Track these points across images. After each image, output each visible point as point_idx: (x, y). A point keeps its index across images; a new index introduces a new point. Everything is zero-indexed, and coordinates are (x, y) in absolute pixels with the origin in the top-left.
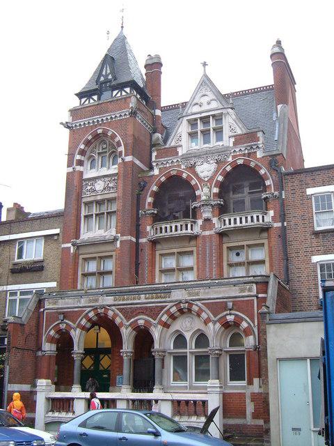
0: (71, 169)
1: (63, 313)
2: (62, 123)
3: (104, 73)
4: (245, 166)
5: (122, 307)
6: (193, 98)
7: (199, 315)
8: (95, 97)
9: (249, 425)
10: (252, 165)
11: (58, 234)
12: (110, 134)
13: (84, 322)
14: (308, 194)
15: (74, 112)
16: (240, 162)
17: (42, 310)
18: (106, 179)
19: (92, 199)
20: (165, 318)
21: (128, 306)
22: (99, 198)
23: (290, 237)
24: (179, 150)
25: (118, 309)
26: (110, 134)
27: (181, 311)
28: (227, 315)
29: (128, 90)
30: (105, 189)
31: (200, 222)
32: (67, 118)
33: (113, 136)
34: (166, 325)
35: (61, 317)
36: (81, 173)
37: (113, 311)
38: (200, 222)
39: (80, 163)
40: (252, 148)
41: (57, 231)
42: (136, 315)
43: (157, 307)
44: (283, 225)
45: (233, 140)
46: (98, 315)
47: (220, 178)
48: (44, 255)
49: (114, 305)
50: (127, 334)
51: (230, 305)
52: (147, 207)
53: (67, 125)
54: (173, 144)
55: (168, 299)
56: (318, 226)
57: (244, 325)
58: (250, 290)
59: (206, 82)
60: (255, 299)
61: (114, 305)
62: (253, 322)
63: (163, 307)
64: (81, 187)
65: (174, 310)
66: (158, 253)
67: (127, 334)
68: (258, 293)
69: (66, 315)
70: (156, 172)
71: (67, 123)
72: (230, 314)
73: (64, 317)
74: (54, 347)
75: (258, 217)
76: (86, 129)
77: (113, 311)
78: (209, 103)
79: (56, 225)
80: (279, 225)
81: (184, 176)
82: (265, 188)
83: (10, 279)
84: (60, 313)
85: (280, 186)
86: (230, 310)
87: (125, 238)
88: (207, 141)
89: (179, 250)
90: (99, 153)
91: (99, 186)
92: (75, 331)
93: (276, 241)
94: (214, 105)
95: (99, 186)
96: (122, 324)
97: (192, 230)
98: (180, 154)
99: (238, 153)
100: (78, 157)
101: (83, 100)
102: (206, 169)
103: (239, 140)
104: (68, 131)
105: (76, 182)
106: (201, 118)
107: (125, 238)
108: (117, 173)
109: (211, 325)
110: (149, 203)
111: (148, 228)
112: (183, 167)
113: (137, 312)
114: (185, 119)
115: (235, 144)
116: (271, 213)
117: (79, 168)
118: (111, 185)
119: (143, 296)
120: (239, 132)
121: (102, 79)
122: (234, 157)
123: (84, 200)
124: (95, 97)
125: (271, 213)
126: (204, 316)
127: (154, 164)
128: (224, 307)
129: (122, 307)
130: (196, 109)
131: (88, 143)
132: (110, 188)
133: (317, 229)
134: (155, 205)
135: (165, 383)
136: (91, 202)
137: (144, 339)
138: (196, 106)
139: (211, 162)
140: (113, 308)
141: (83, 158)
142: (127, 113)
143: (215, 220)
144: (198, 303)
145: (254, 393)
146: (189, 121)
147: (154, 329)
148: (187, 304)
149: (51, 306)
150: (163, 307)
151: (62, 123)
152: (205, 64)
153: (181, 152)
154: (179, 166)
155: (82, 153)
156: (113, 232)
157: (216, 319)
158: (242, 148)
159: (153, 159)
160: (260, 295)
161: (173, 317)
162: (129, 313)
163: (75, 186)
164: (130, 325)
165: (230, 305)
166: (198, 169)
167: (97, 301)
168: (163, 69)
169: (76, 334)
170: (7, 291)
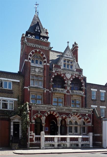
4: (78, 78)
7: (78, 116)
11: (19, 82)
13: (46, 115)
19: (34, 74)
21: (60, 112)
22: (37, 74)
23: (87, 99)
24: (61, 67)
26: (41, 53)
33: (43, 55)
35: (39, 112)
37: (56, 112)
38: (66, 90)
41: (19, 81)
42: (63, 115)
45: (76, 69)
47: (72, 79)
49: (56, 111)
54: (59, 64)
57: (89, 120)
58: (91, 112)
61: (56, 111)
63: (70, 113)
65: (73, 114)
66: (53, 96)
67: (60, 119)
77: (56, 112)
80: (85, 96)
81: (62, 75)
82: (82, 86)
87: (47, 90)
88: (68, 67)
89: (59, 97)
91: (37, 70)
92: (43, 117)
93: (84, 100)
98: (61, 68)
102: (68, 76)
107: (47, 90)
114: (63, 58)
122: (75, 75)
123: (31, 73)
126: (80, 117)
130: (65, 56)
133: (92, 99)
134: (53, 81)
136: (34, 75)
141: (31, 58)
146: (64, 59)
149: (34, 108)
154: (61, 72)
158: (77, 73)
159: (53, 67)
160: (92, 113)
161: (72, 116)
162: (61, 114)
166: (66, 75)
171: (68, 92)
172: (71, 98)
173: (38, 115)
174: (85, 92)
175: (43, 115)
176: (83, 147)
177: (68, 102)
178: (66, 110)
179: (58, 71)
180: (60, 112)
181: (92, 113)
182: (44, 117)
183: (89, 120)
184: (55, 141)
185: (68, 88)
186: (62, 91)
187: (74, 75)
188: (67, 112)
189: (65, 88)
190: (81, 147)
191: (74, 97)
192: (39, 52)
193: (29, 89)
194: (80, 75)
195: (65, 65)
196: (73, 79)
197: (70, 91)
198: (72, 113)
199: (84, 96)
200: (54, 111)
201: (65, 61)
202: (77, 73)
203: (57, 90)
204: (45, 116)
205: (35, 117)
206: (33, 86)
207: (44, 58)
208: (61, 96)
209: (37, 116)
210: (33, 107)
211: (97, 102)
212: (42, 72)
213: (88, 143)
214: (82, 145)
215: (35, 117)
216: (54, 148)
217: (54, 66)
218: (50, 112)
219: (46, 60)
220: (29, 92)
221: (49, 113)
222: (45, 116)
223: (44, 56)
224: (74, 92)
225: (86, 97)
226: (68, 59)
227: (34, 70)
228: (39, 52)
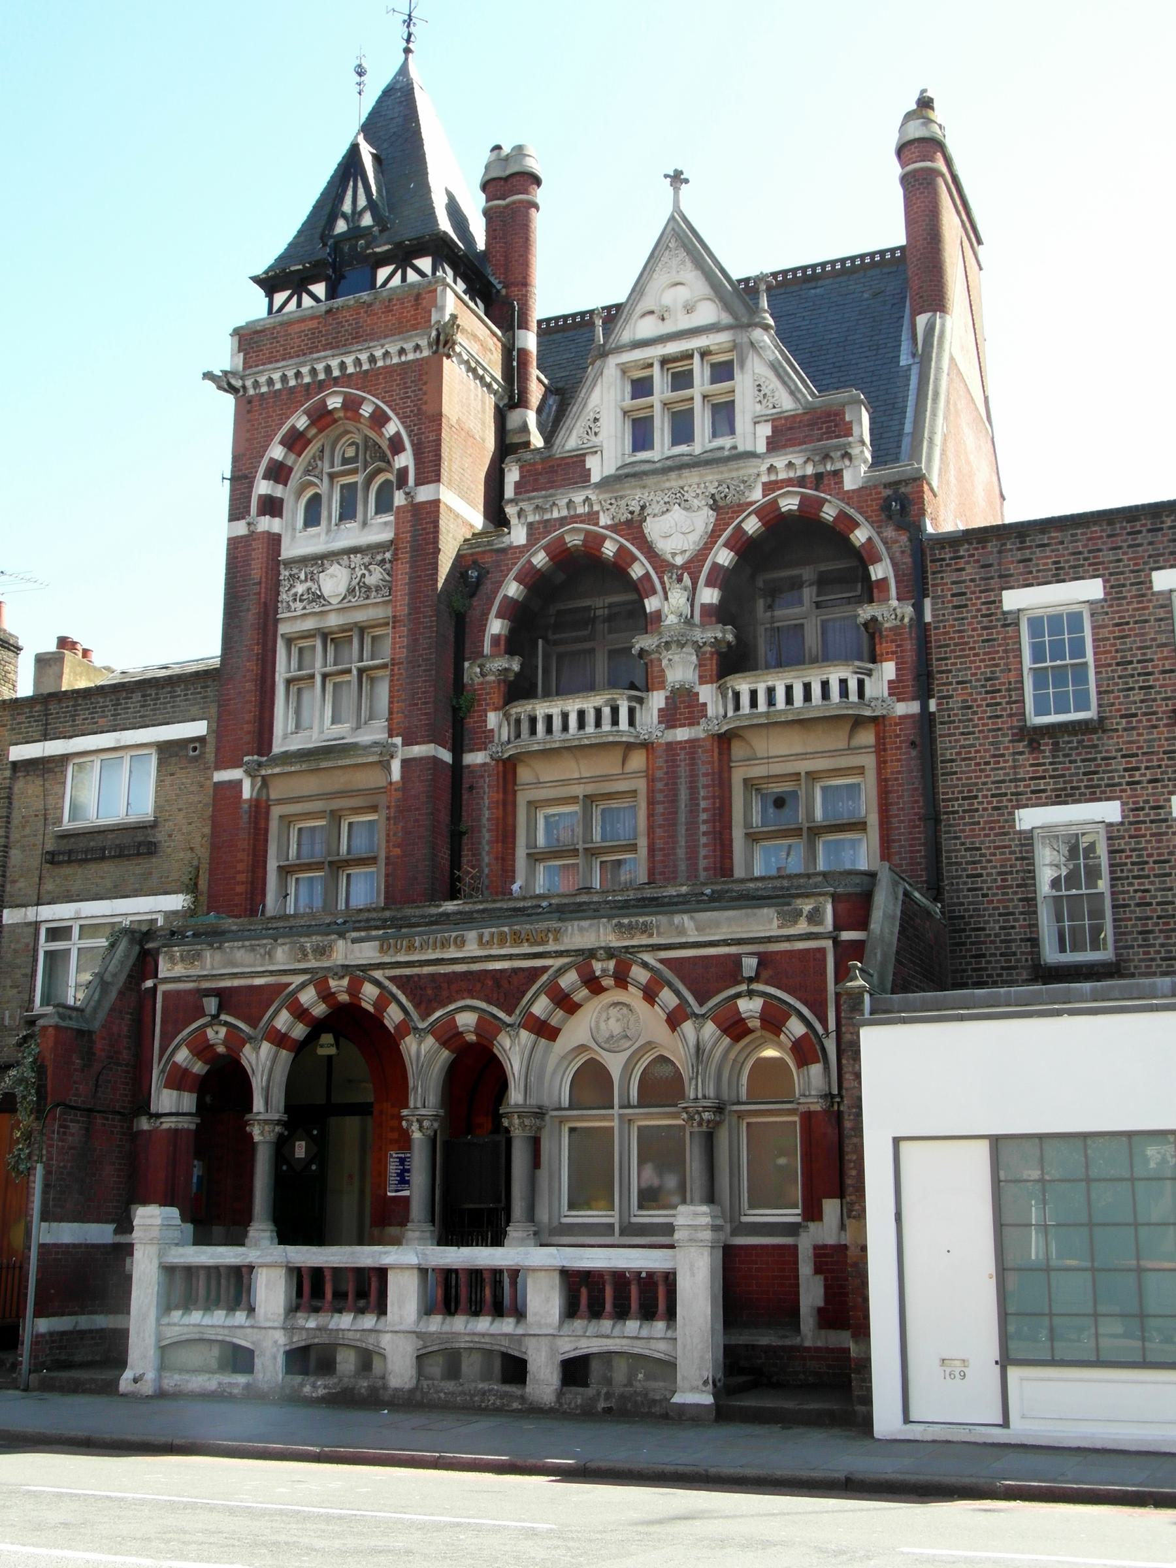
0: (241, 528)
1: (219, 993)
2: (208, 376)
3: (347, 207)
6: (638, 289)
8: (319, 289)
9: (808, 1349)
10: (829, 513)
11: (201, 740)
12: (366, 410)
13: (283, 1021)
14: (1006, 608)
15: (248, 340)
16: (789, 504)
17: (149, 983)
18: (357, 559)
19: (309, 624)
20: (541, 1007)
21: (426, 970)
22: (333, 621)
23: (947, 747)
24: (592, 463)
28: (739, 995)
29: (425, 264)
30: (351, 591)
31: (657, 700)
32: (224, 358)
34: (546, 1031)
35: (211, 1005)
36: (274, 541)
37: (377, 983)
38: (657, 700)
39: (272, 506)
41: (198, 728)
43: (515, 971)
44: (924, 707)
45: (766, 430)
47: (724, 557)
48: (158, 807)
50: (423, 1054)
51: (750, 965)
52: (487, 649)
53: (225, 382)
55: (551, 947)
56: (1041, 711)
57: (796, 1028)
58: (815, 917)
59: (681, 241)
60: (828, 944)
62: (824, 1021)
63: (536, 973)
64: (274, 587)
65: (570, 980)
68: (838, 926)
69: (227, 999)
70: (518, 535)
71: (225, 373)
72: (751, 994)
73: (221, 1008)
74: (188, 1102)
75: (843, 683)
76: (289, 398)
77: (377, 983)
78: (689, 309)
79: (194, 710)
80: (914, 707)
81: (609, 549)
82: (871, 591)
83: (49, 886)
84: (208, 993)
85: (916, 585)
86: (751, 980)
87: (418, 751)
90: (332, 476)
91: (334, 582)
92: (257, 1049)
94: (708, 313)
95: (334, 582)
96: (405, 1028)
97: (632, 723)
98: (595, 478)
99: (782, 476)
100: (263, 487)
101: (280, 298)
102: (678, 530)
103: (785, 433)
104: (228, 401)
105: (257, 571)
106: (665, 361)
107: (418, 751)
108: (392, 541)
109: (688, 1027)
110: (496, 639)
111: (493, 719)
112: (604, 520)
114: (613, 361)
115: (774, 445)
116: (889, 670)
117: (267, 524)
118: (371, 580)
119: (472, 935)
120: (787, 404)
121: (341, 226)
122: (769, 487)
123: (283, 629)
124: (319, 289)
125: (889, 670)
127: (511, 511)
128: (729, 971)
129: (407, 971)
130: (646, 328)
131: (296, 441)
132: (369, 588)
134: (512, 644)
135: (543, 1215)
137: (476, 1076)
138: (650, 319)
139: (696, 502)
140: (378, 974)
141: (278, 491)
142: (423, 343)
143: (707, 693)
144: (647, 957)
145: (825, 1247)
146: (624, 369)
147: (507, 1043)
149: (179, 970)
151: (208, 376)
152: (677, 179)
153: (598, 469)
154: (592, 517)
155: (278, 472)
156: (375, 733)
157: (703, 1010)
158: (793, 463)
159: (509, 492)
160: (846, 935)
161: (567, 1004)
162: (428, 991)
163: (254, 585)
164: (431, 1030)
165: (750, 965)
166: (654, 529)
167: (321, 951)
168: (540, 195)
169: (263, 1063)
170: (36, 925)
171: (682, 707)
172: (738, 776)
173: (210, 1033)
174: (910, 656)
175: (254, 1024)
176: (577, 1396)
177: (682, 830)
178: (490, 943)
179: (563, 521)
180: (426, 970)
181: (846, 935)
182: (266, 1047)
183: (796, 1028)
184: (261, 1310)
185: (680, 669)
186: (591, 718)
187: (757, 495)
188: (498, 965)
189: (638, 678)
190: (560, 1394)
191: (774, 756)
192: (352, 405)
193: (253, 786)
194: (838, 474)
195: (641, 434)
196: (745, 547)
197: (707, 693)
198: (562, 971)
199: (908, 708)
200: (358, 974)
201: (642, 387)
202: (780, 462)
203: (540, 727)
204: (280, 1040)
205: (182, 1056)
206: (295, 745)
207: (396, 445)
208: (606, 778)
209: (202, 1049)
210: (172, 959)
211: (1109, 744)
212: (378, 589)
213: (659, 1349)
214: (575, 1370)
215: (182, 1056)
216: (247, 1386)
217: (518, 485)
218: (326, 995)
219: (405, 460)
220: (260, 809)
221: (308, 997)
222: (280, 1040)
223: (393, 427)
224: (745, 700)
225: (926, 720)
226: (672, 348)
227: (309, 589)
228: (352, 405)
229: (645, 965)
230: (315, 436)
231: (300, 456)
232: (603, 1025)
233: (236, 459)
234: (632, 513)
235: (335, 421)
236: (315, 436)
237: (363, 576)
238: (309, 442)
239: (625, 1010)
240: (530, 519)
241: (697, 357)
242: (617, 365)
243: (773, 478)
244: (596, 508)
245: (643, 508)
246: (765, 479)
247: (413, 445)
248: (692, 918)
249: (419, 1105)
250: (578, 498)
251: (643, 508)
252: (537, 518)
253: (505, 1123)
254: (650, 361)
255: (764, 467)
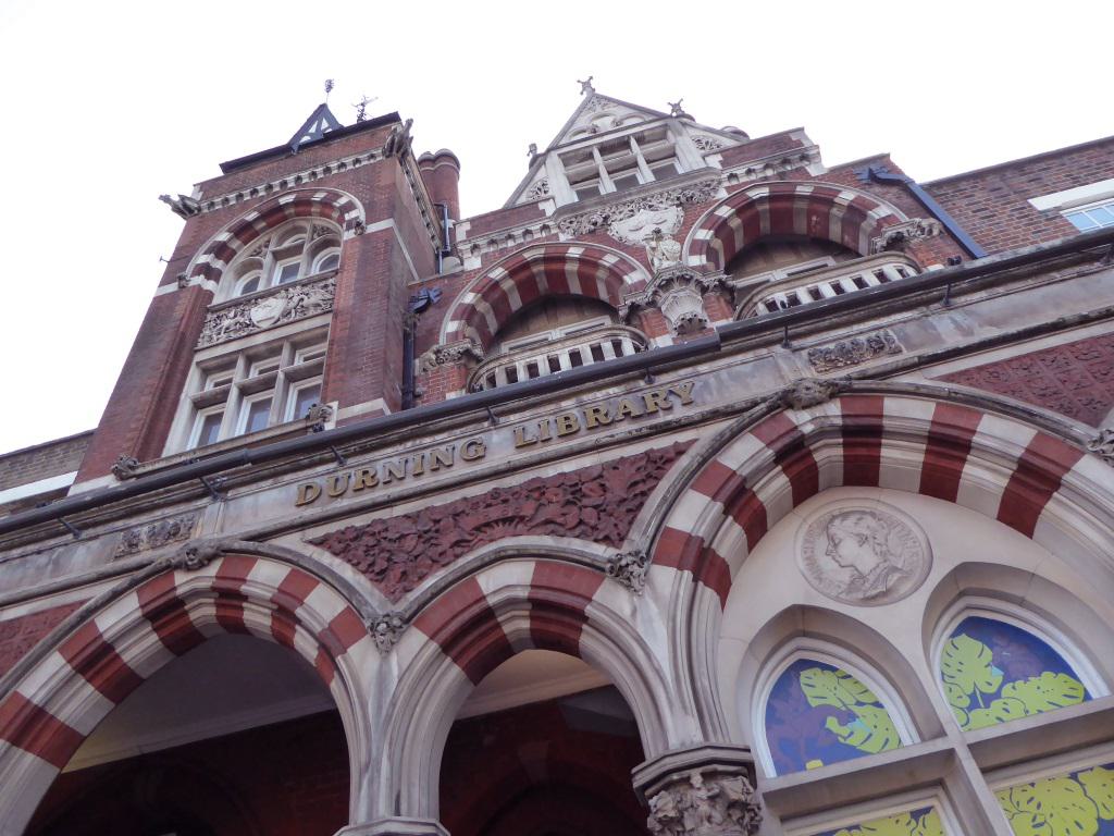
2: (166, 199)
5: (359, 521)
20: (693, 514)
25: (320, 543)
27: (794, 455)
40: (786, 161)
42: (462, 545)
46: (164, 613)
63: (658, 463)
71: (183, 198)
98: (549, 212)
113: (469, 522)
140: (291, 542)
148: (834, 410)
150: (658, 463)
151: (166, 199)
155: (222, 251)
188: (569, 466)
202: (740, 171)
229: (916, 393)
230: (263, 230)
231: (245, 243)
232: (827, 564)
233: (178, 250)
234: (595, 224)
235: (285, 218)
236: (263, 230)
237: (302, 299)
238: (257, 234)
239: (869, 520)
240: (484, 251)
241: (633, 142)
242: (559, 155)
243: (734, 182)
244: (554, 231)
245: (606, 219)
246: (726, 184)
247: (364, 205)
248: (969, 314)
249: (383, 808)
250: (535, 227)
251: (606, 219)
252: (492, 249)
253: (663, 804)
254: (588, 150)
255: (725, 176)
